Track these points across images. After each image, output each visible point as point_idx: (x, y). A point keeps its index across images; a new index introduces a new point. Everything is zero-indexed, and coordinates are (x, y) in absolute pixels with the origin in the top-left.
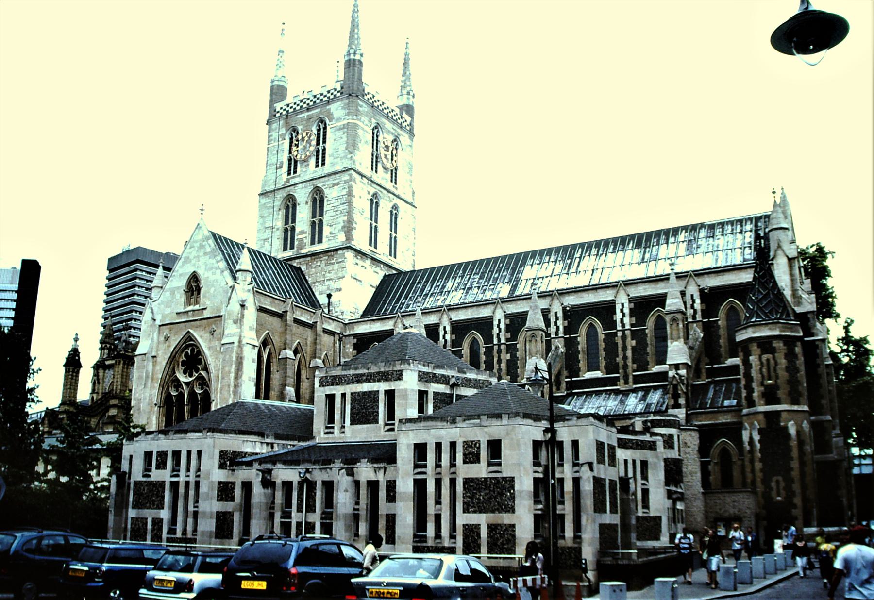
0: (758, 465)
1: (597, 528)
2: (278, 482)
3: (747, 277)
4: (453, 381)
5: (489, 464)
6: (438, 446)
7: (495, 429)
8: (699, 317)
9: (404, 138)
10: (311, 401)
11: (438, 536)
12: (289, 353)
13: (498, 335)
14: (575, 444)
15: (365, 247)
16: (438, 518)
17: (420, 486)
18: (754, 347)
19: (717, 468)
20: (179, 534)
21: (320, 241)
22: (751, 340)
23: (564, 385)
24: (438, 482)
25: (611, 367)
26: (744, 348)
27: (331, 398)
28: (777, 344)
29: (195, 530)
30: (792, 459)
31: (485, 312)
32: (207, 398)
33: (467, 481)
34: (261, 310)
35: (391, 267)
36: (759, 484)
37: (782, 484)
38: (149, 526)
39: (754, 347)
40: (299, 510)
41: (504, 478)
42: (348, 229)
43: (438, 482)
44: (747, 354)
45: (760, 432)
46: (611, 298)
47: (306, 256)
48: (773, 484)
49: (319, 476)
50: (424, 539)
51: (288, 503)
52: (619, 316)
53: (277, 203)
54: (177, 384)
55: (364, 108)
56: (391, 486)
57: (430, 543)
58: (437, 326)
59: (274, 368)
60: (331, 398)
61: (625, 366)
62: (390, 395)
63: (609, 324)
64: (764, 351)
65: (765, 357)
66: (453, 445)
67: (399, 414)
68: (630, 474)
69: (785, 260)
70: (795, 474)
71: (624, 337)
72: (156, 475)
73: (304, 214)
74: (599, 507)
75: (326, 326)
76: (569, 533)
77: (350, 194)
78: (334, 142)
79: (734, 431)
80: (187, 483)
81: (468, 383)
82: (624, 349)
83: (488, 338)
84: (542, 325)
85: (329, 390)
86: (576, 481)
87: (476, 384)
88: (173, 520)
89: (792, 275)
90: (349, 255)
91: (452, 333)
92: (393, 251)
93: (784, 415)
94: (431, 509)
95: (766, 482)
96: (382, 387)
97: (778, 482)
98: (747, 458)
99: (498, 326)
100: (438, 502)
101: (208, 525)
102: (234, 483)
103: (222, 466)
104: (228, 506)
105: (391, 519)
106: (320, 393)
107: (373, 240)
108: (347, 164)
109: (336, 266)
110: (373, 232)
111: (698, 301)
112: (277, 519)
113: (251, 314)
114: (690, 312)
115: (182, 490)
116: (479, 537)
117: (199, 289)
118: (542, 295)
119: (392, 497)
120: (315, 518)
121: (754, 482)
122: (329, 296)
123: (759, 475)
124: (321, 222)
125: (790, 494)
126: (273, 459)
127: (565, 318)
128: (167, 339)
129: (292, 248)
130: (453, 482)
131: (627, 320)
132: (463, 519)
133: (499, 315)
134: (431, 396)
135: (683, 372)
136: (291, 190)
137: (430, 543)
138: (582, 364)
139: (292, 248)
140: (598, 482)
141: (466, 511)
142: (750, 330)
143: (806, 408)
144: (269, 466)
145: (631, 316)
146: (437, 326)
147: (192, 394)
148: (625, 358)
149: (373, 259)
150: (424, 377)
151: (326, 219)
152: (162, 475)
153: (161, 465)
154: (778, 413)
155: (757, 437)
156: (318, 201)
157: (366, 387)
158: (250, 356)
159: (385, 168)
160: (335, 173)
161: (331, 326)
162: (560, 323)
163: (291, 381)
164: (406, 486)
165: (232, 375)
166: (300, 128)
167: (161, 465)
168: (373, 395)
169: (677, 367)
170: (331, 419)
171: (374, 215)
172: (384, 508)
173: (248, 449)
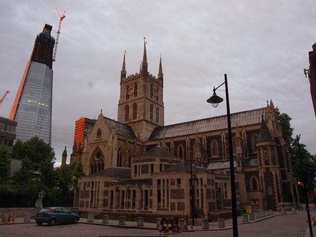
0: (264, 184)
1: (208, 204)
2: (121, 191)
3: (259, 127)
4: (170, 161)
5: (177, 185)
6: (164, 180)
7: (178, 176)
8: (246, 139)
9: (160, 88)
10: (130, 167)
11: (164, 206)
12: (127, 151)
14: (201, 179)
15: (149, 120)
16: (164, 200)
17: (159, 191)
18: (261, 148)
19: (252, 184)
21: (136, 119)
22: (261, 146)
23: (207, 160)
24: (164, 190)
25: (221, 154)
26: (258, 147)
27: (136, 166)
28: (268, 147)
29: (98, 204)
30: (274, 182)
31: (183, 138)
32: (103, 165)
33: (172, 190)
34: (119, 139)
35: (157, 125)
36: (264, 189)
37: (271, 190)
38: (85, 203)
39: (261, 148)
40: (126, 198)
42: (144, 115)
43: (164, 190)
44: (259, 150)
45: (264, 173)
46: (220, 134)
47: (132, 123)
48: (269, 189)
49: (132, 189)
50: (160, 207)
51: (123, 197)
52: (222, 139)
53: (124, 107)
54: (95, 161)
55: (148, 80)
56: (151, 191)
57: (162, 208)
58: (170, 142)
59: (122, 155)
60: (136, 166)
61: (225, 154)
62: (152, 165)
63: (220, 142)
64: (265, 149)
65: (264, 151)
66: (168, 180)
67: (155, 171)
68: (221, 187)
69: (271, 122)
70: (275, 186)
71: (224, 146)
72: (87, 189)
73: (131, 111)
74: (208, 197)
75: (138, 143)
76: (200, 205)
77: (144, 105)
78: (140, 90)
79: (257, 173)
80: (96, 191)
81: (174, 161)
82: (224, 149)
83: (185, 146)
84: (200, 142)
85: (135, 164)
86: (202, 190)
87: (177, 162)
88: (92, 202)
89: (273, 126)
90: (144, 122)
91: (174, 144)
92: (157, 121)
93: (271, 169)
94: (162, 198)
95: (266, 188)
96: (149, 163)
97: (270, 189)
98: (260, 182)
100: (164, 196)
101: (101, 203)
102: (108, 191)
103: (105, 186)
105: (151, 201)
106: (133, 165)
107: (151, 118)
108: (144, 96)
109: (140, 126)
110: (152, 115)
111: (245, 134)
112: (120, 201)
113: (116, 140)
114: (243, 138)
115: (94, 193)
116: (175, 206)
117: (101, 134)
118: (200, 133)
119: (151, 195)
120: (131, 201)
121: (263, 189)
122: (139, 134)
123: (264, 187)
124: (136, 113)
125: (274, 192)
126: (118, 184)
127: (207, 140)
128: (92, 148)
129: (128, 120)
130: (168, 190)
131: (225, 141)
133: (188, 139)
134: (163, 165)
135: (241, 156)
136: (127, 104)
137: (162, 208)
138: (212, 154)
139: (128, 120)
140: (208, 191)
142: (260, 143)
143: (278, 166)
144: (118, 186)
145: (226, 139)
146: (170, 142)
147: (99, 164)
148: (224, 151)
149: (151, 123)
150: (161, 160)
151: (138, 112)
152: (89, 189)
153: (89, 186)
154: (269, 168)
155: (263, 175)
156: (135, 106)
157: (145, 163)
158: (116, 152)
159: (155, 97)
160: (140, 98)
161: (139, 143)
162: (205, 141)
163: (128, 159)
164: (155, 191)
165: (110, 159)
166: (130, 85)
167: (89, 186)
168: (147, 166)
169: (239, 154)
170: (136, 172)
171: (151, 111)
172: (149, 198)
173: (113, 181)
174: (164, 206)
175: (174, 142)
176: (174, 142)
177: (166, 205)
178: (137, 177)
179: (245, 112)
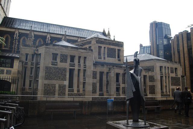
11: (166, 92)
13: (48, 41)
20: (75, 92)
24: (166, 77)
31: (46, 34)
33: (172, 77)
41: (178, 77)
57: (165, 93)
62: (119, 50)
72: (61, 65)
80: (79, 70)
85: (100, 45)
88: (71, 85)
94: (165, 84)
99: (48, 39)
100: (166, 83)
101: (89, 88)
102: (96, 72)
104: (95, 81)
115: (76, 73)
130: (169, 77)
132: (171, 87)
133: (48, 36)
137: (165, 93)
141: (172, 85)
152: (66, 65)
157: (112, 47)
174: (166, 92)
175: (35, 35)
176: (35, 35)
177: (168, 91)
178: (102, 59)
179: (89, 30)
